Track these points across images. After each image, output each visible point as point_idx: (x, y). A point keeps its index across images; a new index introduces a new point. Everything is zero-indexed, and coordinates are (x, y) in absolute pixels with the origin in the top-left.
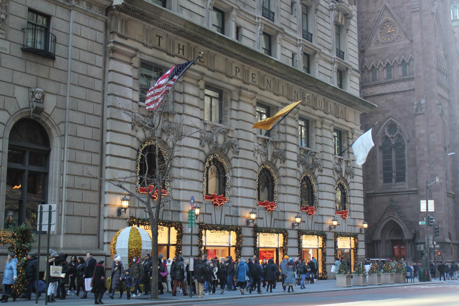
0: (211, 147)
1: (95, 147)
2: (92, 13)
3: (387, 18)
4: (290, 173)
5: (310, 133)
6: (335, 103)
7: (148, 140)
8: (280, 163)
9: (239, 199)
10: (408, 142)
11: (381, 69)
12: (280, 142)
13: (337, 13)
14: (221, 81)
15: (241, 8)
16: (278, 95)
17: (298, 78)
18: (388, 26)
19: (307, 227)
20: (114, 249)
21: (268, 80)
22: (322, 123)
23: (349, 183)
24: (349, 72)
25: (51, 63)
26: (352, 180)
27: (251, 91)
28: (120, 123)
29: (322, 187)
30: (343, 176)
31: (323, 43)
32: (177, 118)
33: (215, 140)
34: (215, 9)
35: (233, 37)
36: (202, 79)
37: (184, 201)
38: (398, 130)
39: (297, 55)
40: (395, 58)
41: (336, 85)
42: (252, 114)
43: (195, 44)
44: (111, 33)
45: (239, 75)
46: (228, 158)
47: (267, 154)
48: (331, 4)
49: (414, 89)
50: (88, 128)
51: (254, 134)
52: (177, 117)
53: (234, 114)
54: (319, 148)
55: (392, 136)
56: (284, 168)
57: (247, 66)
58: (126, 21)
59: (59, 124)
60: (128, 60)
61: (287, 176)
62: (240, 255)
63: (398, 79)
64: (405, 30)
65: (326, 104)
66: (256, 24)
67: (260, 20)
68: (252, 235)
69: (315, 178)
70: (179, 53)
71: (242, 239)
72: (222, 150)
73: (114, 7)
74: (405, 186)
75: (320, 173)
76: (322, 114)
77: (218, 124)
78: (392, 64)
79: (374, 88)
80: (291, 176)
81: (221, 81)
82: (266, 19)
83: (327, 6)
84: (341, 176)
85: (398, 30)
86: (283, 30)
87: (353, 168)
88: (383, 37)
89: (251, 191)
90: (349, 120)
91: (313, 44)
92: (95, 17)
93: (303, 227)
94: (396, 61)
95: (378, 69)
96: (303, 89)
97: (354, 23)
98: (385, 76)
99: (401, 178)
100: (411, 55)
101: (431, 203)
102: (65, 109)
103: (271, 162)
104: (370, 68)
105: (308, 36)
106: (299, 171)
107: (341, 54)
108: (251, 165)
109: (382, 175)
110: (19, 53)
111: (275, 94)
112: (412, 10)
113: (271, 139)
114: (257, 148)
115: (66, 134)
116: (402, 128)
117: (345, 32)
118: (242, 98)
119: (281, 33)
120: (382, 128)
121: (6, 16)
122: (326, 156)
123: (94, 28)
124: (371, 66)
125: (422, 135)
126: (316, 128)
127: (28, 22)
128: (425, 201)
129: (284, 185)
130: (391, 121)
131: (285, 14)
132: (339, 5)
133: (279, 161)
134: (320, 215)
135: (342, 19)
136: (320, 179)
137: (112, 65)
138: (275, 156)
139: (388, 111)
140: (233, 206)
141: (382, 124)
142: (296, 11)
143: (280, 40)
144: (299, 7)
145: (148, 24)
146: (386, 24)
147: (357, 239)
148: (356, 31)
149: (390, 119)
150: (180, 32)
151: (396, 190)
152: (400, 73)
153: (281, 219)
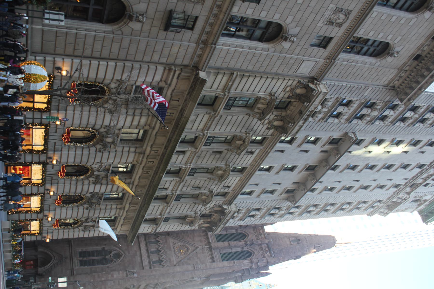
0: (104, 133)
1: (105, 54)
2: (194, 57)
3: (190, 249)
4: (86, 188)
5: (113, 201)
6: (134, 217)
7: (110, 90)
8: (92, 181)
9: (67, 152)
10: (108, 267)
11: (157, 246)
12: (107, 180)
13: (193, 217)
14: (149, 140)
15: (197, 154)
16: (139, 179)
17: (151, 192)
18: (185, 250)
19: (47, 199)
20: (31, 64)
22: (120, 209)
23: (79, 228)
24: (155, 226)
25: (162, 28)
26: (81, 230)
27: (142, 161)
28: (121, 71)
29: (75, 210)
30: (84, 224)
31: (174, 208)
32: (124, 111)
33: (109, 136)
34: (196, 137)
35: (178, 149)
36: (150, 128)
37: (66, 114)
38: (116, 260)
39: (166, 191)
40: (164, 256)
41: (146, 217)
42: (126, 161)
43: (174, 124)
44: (181, 69)
45: (153, 152)
46: (96, 145)
48: (199, 213)
49: (143, 269)
50: (118, 50)
51: (113, 163)
52: (125, 111)
53: (126, 149)
54: (103, 207)
55: (112, 256)
56: (89, 183)
57: (159, 158)
58: (189, 79)
59: (121, 31)
60: (164, 79)
61: (83, 185)
62: (26, 153)
63: (151, 258)
64: (182, 261)
65: (133, 211)
66: (186, 164)
67: (189, 167)
68: (41, 161)
69: (82, 205)
70: (168, 113)
71: (38, 154)
72: (102, 141)
73: (198, 72)
74: (77, 266)
75: (85, 208)
76: (126, 209)
77: (119, 138)
78: (160, 253)
79: (144, 242)
81: (149, 140)
82: (189, 170)
83: (198, 210)
84: (84, 223)
85: (182, 256)
86: (183, 181)
87: (89, 231)
88: (178, 247)
89: (73, 160)
90: (122, 227)
91: (173, 202)
92: (192, 59)
93: (47, 197)
94: (162, 256)
95: (157, 245)
96: (144, 195)
97: (187, 228)
98: (153, 250)
99: (82, 263)
100: (166, 266)
101: (65, 285)
102: (131, 36)
103: (93, 174)
104: (157, 239)
105: (178, 198)
106: (87, 193)
107: (167, 220)
108: (91, 160)
109: (84, 250)
110: (169, 8)
111: (140, 177)
112: (195, 265)
113: (109, 174)
114: (103, 164)
115: (115, 35)
116: (117, 263)
117: (181, 222)
118: (137, 154)
119: (180, 181)
120: (117, 249)
121: (193, 2)
122: (97, 212)
123: (185, 58)
124: (159, 240)
125: (112, 276)
126: (117, 205)
127: (189, 16)
128: (66, 281)
129: (77, 183)
130: (122, 255)
131: (192, 183)
132: (198, 218)
133: (94, 179)
134: (55, 208)
135: (190, 220)
137: (161, 69)
138: (97, 177)
139: (129, 253)
140: (62, 148)
141: (120, 249)
142: (194, 190)
143: (176, 180)
144: (197, 192)
145: (186, 93)
146: (186, 248)
147: (38, 235)
148: (182, 229)
149: (124, 254)
150: (181, 114)
151: (74, 261)
152: (154, 260)
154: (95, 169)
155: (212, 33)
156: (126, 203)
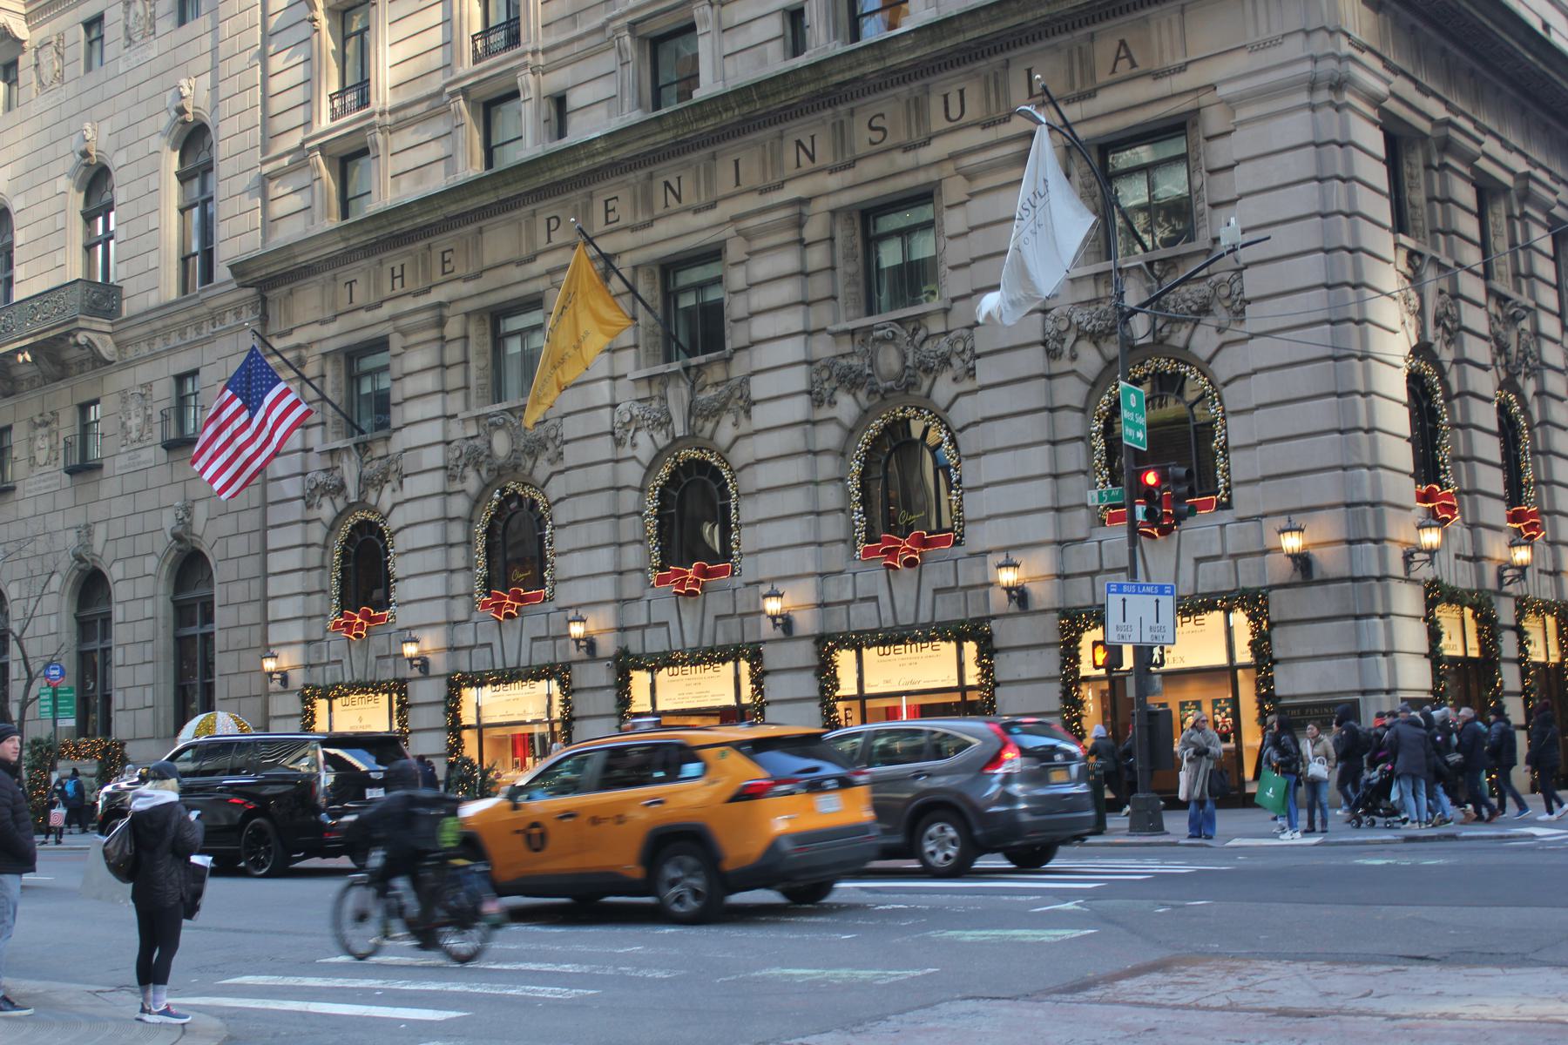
0: (484, 472)
8: (735, 425)
19: (886, 613)
21: (667, 184)
47: (671, 420)
57: (577, 196)
75: (967, 385)
80: (778, 454)
90: (1181, 60)
96: (829, 112)
136: (962, 413)
153: (745, 610)
154: (662, 439)
155: (193, 318)
156: (917, 168)
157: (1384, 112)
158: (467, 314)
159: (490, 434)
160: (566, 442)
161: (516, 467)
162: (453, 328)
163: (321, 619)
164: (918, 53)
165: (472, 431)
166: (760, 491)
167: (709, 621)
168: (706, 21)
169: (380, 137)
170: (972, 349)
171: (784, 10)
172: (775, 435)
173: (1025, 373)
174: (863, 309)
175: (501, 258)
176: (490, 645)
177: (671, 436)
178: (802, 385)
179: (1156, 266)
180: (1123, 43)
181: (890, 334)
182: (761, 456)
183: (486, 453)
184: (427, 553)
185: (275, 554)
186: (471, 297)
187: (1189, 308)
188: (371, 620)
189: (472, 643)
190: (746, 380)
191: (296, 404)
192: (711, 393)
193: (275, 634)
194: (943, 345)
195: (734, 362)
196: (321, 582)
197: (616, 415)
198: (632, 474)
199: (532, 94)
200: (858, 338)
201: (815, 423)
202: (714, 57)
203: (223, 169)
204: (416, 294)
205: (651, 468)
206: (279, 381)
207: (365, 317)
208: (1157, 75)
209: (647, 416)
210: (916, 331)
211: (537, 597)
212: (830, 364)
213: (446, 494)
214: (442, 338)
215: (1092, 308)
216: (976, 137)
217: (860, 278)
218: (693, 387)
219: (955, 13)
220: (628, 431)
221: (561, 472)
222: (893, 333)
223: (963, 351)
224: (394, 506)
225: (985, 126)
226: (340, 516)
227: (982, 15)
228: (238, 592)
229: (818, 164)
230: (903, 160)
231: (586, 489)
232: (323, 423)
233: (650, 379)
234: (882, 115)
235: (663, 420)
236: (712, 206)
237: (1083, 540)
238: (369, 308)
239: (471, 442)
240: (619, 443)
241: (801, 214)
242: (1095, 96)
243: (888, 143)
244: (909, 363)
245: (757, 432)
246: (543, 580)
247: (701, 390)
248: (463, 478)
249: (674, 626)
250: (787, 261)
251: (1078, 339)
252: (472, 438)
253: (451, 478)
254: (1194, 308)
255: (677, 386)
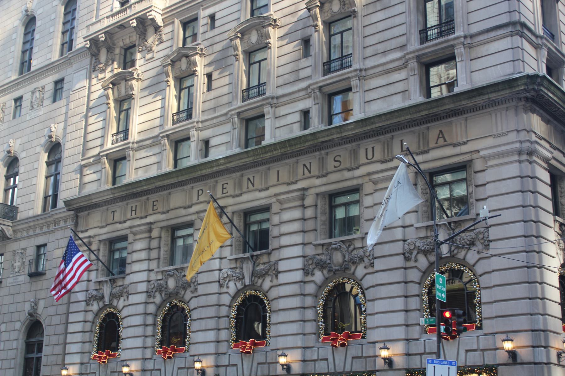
0: (163, 295)
8: (271, 281)
19: (331, 366)
21: (249, 179)
47: (244, 277)
57: (211, 181)
75: (370, 270)
80: (289, 294)
90: (465, 140)
119: (268, 103)
136: (368, 281)
153: (271, 361)
154: (239, 285)
155: (46, 222)
156: (353, 178)
157: (550, 165)
158: (162, 228)
159: (167, 279)
160: (199, 284)
161: (177, 294)
162: (155, 233)
163: (88, 354)
164: (356, 131)
165: (160, 277)
166: (280, 310)
167: (255, 365)
168: (269, 113)
169: (131, 153)
170: (373, 255)
171: (302, 111)
172: (288, 287)
173: (395, 266)
174: (328, 236)
175: (178, 205)
176: (160, 370)
177: (243, 284)
178: (300, 266)
179: (452, 224)
180: (441, 131)
181: (339, 247)
182: (281, 295)
183: (165, 287)
184: (136, 328)
185: (71, 324)
186: (163, 221)
187: (466, 242)
188: (110, 355)
189: (152, 368)
190: (277, 263)
191: (86, 261)
192: (262, 267)
193: (68, 359)
194: (361, 252)
195: (272, 254)
196: (90, 338)
197: (221, 274)
198: (226, 299)
199: (195, 139)
200: (325, 247)
201: (305, 282)
202: (271, 128)
203: (65, 161)
204: (141, 218)
205: (234, 298)
206: (79, 251)
207: (119, 226)
208: (455, 145)
209: (234, 275)
210: (349, 246)
211: (182, 350)
212: (313, 258)
213: (147, 303)
214: (150, 237)
215: (424, 240)
216: (379, 166)
217: (327, 223)
218: (254, 264)
219: (372, 116)
220: (225, 281)
221: (196, 297)
222: (340, 246)
223: (369, 256)
224: (124, 307)
225: (382, 162)
226: (101, 310)
227: (383, 117)
228: (54, 340)
229: (312, 174)
230: (347, 174)
231: (206, 305)
232: (97, 270)
233: (236, 260)
234: (340, 156)
235: (240, 277)
236: (267, 189)
237: (417, 339)
238: (120, 223)
239: (159, 282)
240: (221, 286)
241: (304, 195)
242: (429, 152)
243: (341, 167)
244: (346, 259)
245: (280, 285)
246: (185, 342)
247: (257, 266)
248: (154, 297)
249: (240, 366)
250: (297, 214)
251: (418, 253)
252: (160, 280)
253: (149, 296)
254: (468, 242)
255: (248, 263)
